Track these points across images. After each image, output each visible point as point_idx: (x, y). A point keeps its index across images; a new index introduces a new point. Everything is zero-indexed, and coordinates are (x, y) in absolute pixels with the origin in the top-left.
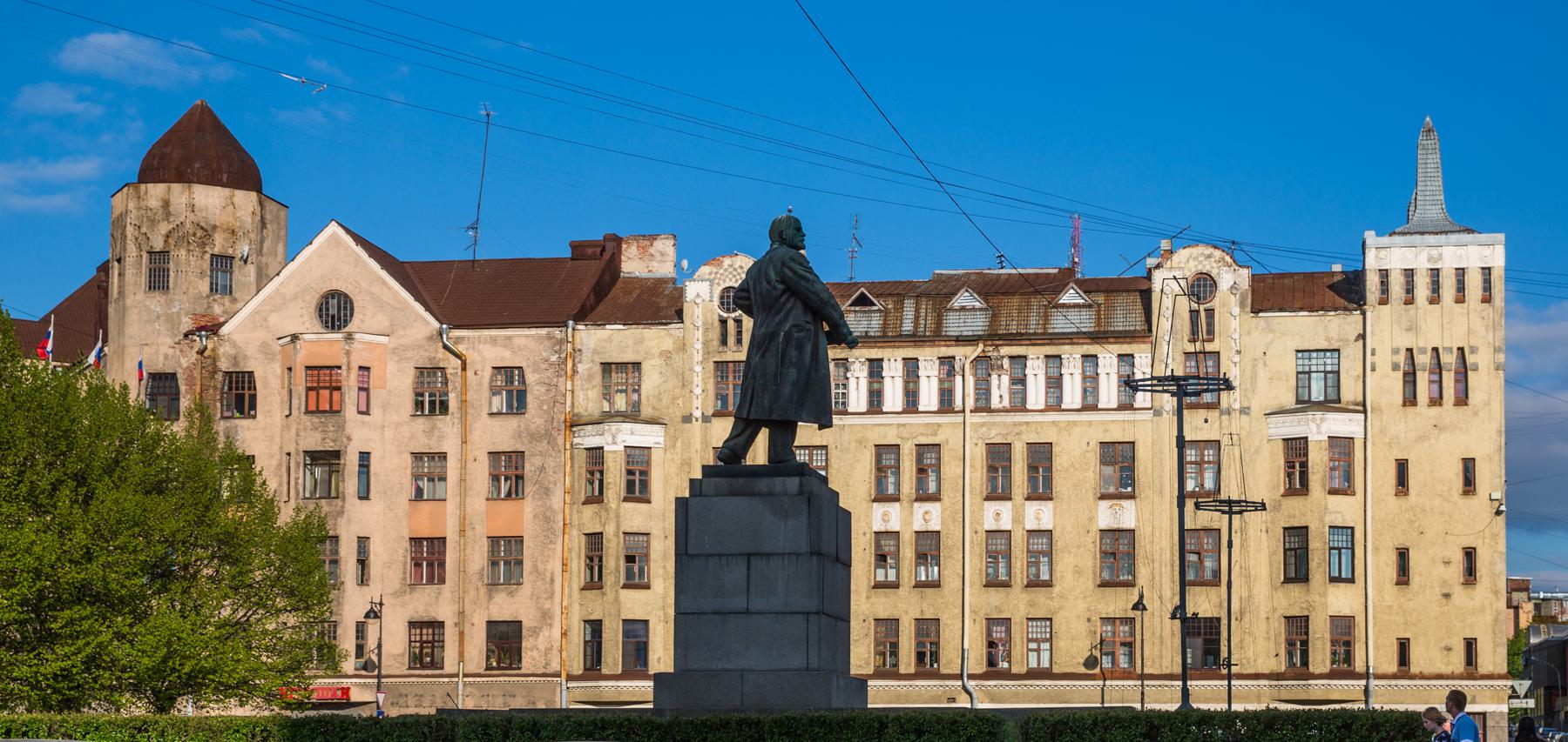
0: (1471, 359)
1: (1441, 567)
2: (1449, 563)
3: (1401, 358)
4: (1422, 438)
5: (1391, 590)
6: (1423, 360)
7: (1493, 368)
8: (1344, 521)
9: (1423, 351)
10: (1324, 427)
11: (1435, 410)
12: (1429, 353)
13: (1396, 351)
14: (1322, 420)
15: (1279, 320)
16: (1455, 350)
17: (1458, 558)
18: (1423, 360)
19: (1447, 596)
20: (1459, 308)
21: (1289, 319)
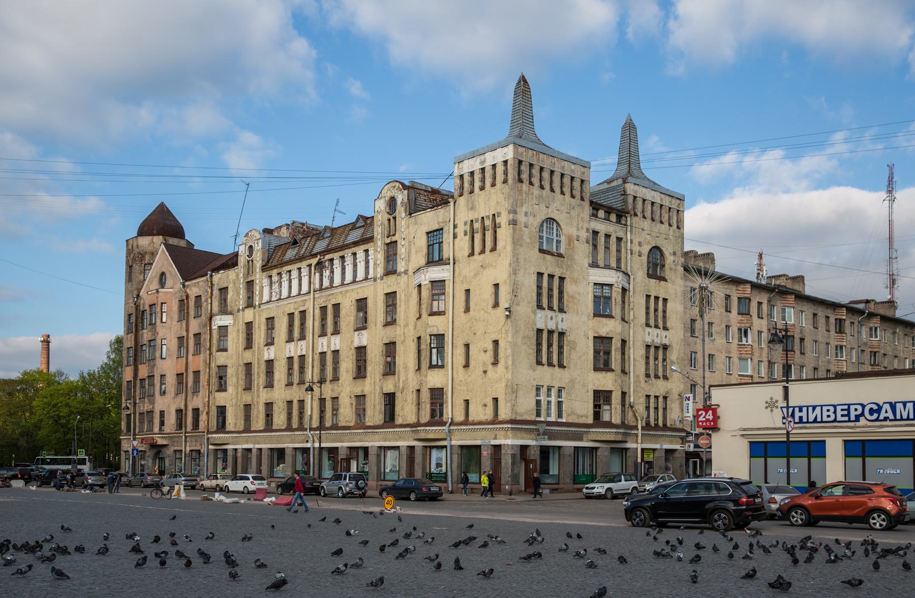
0: (498, 220)
1: (483, 353)
2: (486, 351)
3: (468, 228)
4: (476, 275)
5: (461, 369)
6: (477, 226)
7: (507, 224)
8: (438, 330)
9: (477, 220)
10: (428, 275)
11: (482, 256)
12: (480, 222)
13: (465, 224)
14: (427, 271)
15: (420, 216)
16: (491, 217)
17: (490, 347)
18: (477, 226)
19: (485, 372)
20: (493, 190)
21: (423, 215)
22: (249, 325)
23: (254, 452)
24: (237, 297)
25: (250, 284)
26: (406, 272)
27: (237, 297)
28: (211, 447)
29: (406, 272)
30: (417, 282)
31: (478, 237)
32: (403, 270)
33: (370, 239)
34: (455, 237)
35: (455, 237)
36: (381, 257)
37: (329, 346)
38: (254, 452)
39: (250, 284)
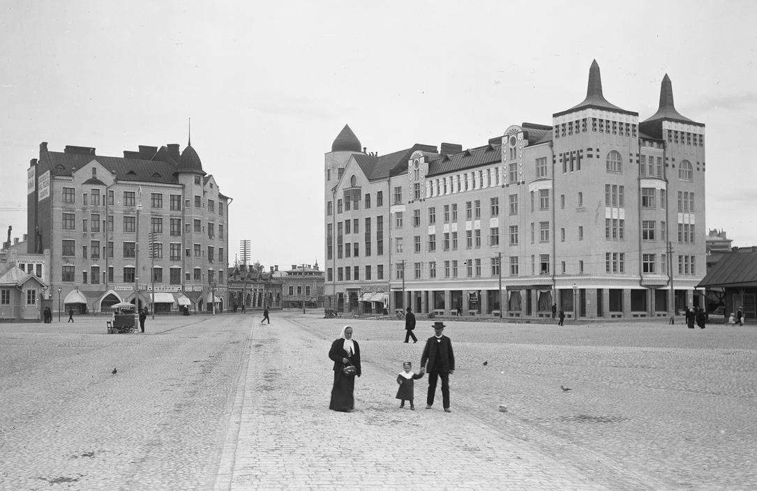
3: (562, 157)
13: (561, 155)
22: (417, 212)
23: (423, 294)
24: (408, 194)
25: (417, 185)
26: (523, 183)
27: (408, 194)
28: (391, 290)
29: (523, 183)
30: (530, 190)
31: (568, 163)
32: (521, 181)
33: (500, 161)
34: (554, 162)
35: (554, 162)
36: (507, 173)
37: (473, 224)
38: (423, 294)
39: (417, 185)
